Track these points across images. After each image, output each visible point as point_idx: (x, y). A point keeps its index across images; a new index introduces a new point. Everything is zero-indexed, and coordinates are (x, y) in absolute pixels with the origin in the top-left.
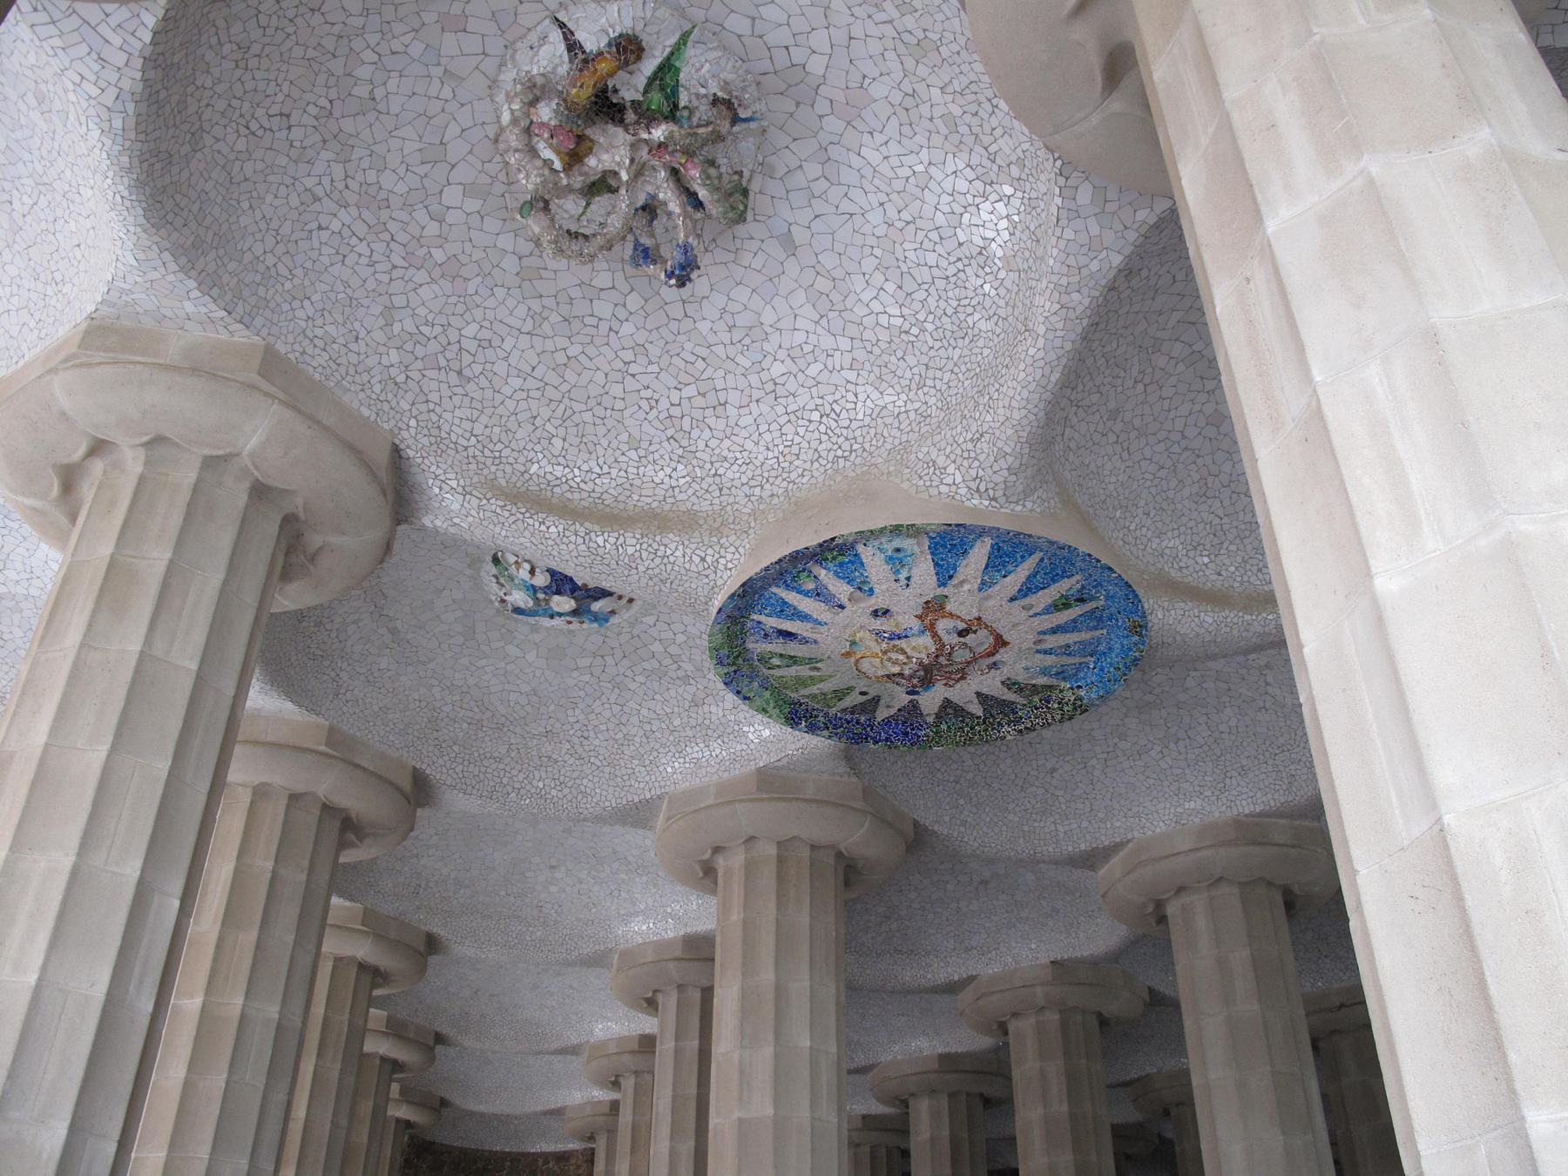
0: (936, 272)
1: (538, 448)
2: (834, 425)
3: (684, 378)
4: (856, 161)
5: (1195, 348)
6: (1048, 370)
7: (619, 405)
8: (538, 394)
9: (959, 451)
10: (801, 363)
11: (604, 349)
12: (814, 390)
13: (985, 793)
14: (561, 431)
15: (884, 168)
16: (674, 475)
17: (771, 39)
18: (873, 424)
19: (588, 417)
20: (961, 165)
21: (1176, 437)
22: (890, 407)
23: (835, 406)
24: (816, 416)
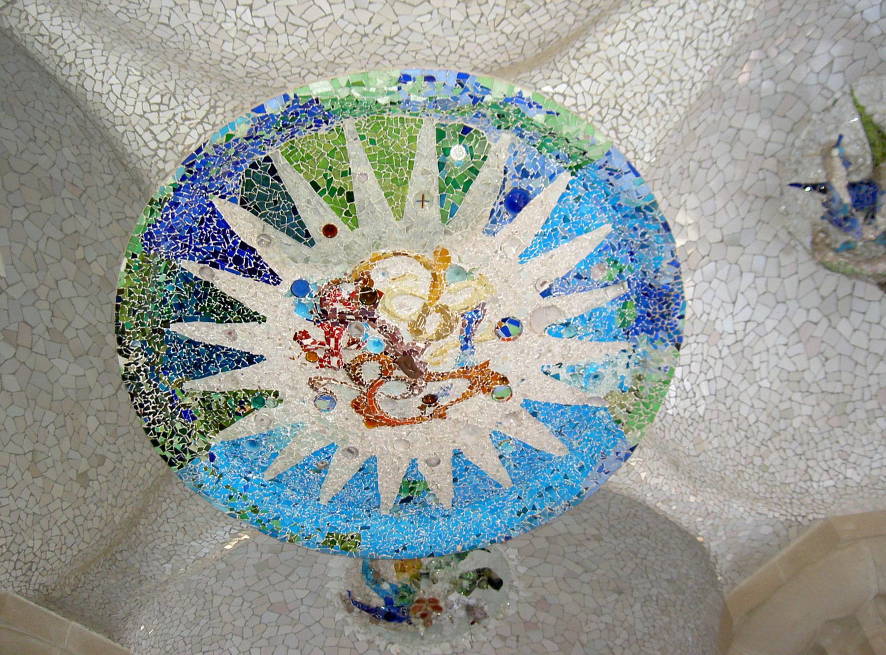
4: (770, 324)
15: (760, 347)
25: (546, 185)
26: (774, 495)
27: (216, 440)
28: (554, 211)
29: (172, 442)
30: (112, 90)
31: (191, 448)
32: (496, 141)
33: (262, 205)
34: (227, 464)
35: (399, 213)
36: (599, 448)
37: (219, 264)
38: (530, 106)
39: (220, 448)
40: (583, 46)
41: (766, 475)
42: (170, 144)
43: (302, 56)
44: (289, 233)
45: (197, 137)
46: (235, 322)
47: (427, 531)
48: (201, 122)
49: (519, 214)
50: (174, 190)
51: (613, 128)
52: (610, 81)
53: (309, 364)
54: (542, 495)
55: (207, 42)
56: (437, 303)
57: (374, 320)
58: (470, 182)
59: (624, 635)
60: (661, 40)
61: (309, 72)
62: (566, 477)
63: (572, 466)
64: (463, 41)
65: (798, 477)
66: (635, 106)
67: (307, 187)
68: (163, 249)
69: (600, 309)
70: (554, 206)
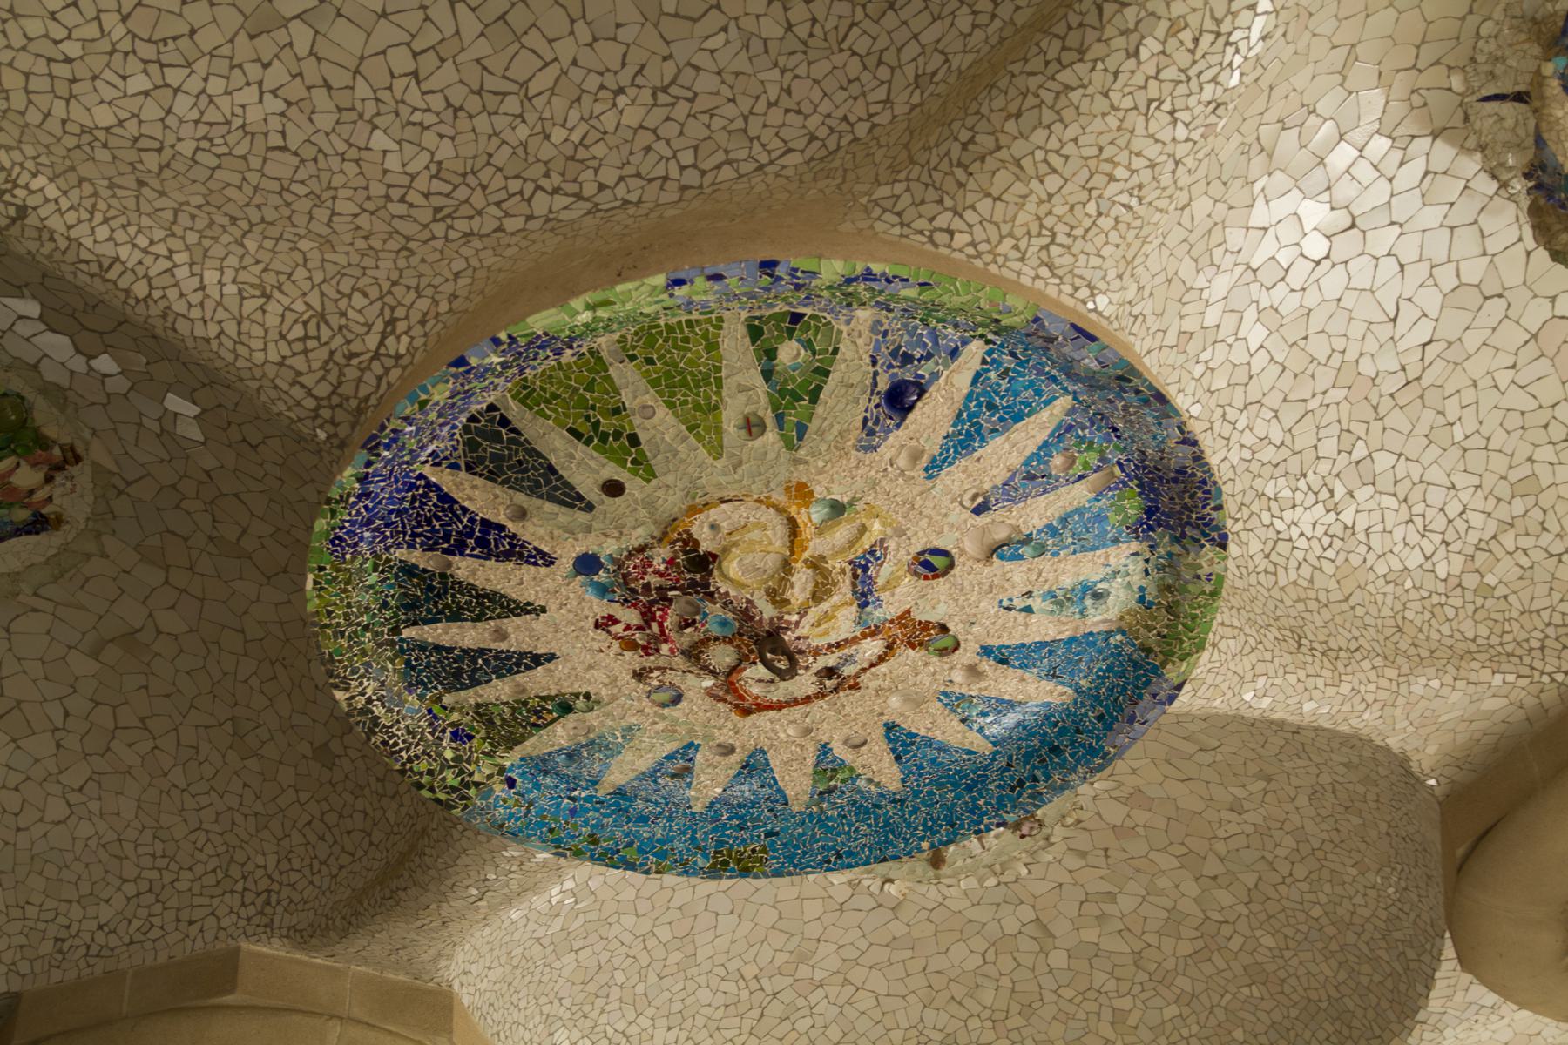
0: (1309, 455)
4: (1472, 340)
20: (1465, 496)
25: (946, 366)
26: (1507, 638)
27: (510, 759)
28: (969, 397)
29: (444, 779)
30: (222, 332)
31: (477, 777)
32: (848, 322)
33: (500, 468)
34: (537, 786)
35: (717, 451)
36: (1124, 688)
37: (460, 549)
38: (888, 281)
39: (520, 767)
40: (972, 140)
41: (1489, 603)
42: (335, 400)
43: (520, 150)
44: (552, 499)
45: (374, 382)
46: (499, 617)
47: (870, 826)
48: (377, 355)
49: (911, 416)
50: (359, 480)
51: (1043, 264)
52: (1024, 197)
53: (628, 654)
54: (1044, 760)
55: (357, 161)
56: (806, 555)
57: (711, 595)
58: (819, 389)
59: (1289, 842)
60: (1104, 115)
61: (538, 188)
62: (1078, 731)
63: (1086, 715)
64: (788, 75)
66: (1074, 223)
67: (563, 437)
68: (363, 546)
69: (1080, 511)
70: (965, 391)
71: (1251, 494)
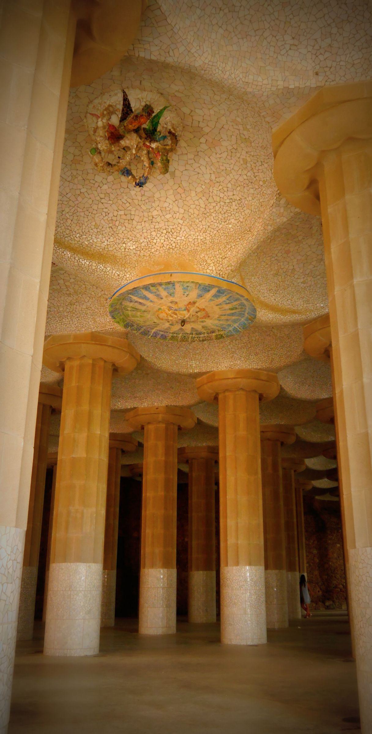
0: (222, 199)
1: (62, 222)
2: (170, 236)
3: (120, 208)
4: (207, 159)
5: (290, 231)
6: (253, 245)
7: (95, 212)
8: (66, 203)
9: (216, 260)
10: (164, 213)
11: (95, 192)
12: (166, 223)
13: (165, 348)
14: (71, 218)
16: (109, 240)
17: (194, 118)
18: (185, 240)
19: (82, 214)
21: (274, 256)
22: (192, 235)
23: (173, 230)
24: (165, 232)
65: (270, 170)
71: (223, 215)
